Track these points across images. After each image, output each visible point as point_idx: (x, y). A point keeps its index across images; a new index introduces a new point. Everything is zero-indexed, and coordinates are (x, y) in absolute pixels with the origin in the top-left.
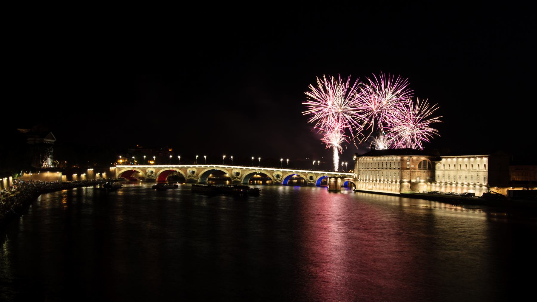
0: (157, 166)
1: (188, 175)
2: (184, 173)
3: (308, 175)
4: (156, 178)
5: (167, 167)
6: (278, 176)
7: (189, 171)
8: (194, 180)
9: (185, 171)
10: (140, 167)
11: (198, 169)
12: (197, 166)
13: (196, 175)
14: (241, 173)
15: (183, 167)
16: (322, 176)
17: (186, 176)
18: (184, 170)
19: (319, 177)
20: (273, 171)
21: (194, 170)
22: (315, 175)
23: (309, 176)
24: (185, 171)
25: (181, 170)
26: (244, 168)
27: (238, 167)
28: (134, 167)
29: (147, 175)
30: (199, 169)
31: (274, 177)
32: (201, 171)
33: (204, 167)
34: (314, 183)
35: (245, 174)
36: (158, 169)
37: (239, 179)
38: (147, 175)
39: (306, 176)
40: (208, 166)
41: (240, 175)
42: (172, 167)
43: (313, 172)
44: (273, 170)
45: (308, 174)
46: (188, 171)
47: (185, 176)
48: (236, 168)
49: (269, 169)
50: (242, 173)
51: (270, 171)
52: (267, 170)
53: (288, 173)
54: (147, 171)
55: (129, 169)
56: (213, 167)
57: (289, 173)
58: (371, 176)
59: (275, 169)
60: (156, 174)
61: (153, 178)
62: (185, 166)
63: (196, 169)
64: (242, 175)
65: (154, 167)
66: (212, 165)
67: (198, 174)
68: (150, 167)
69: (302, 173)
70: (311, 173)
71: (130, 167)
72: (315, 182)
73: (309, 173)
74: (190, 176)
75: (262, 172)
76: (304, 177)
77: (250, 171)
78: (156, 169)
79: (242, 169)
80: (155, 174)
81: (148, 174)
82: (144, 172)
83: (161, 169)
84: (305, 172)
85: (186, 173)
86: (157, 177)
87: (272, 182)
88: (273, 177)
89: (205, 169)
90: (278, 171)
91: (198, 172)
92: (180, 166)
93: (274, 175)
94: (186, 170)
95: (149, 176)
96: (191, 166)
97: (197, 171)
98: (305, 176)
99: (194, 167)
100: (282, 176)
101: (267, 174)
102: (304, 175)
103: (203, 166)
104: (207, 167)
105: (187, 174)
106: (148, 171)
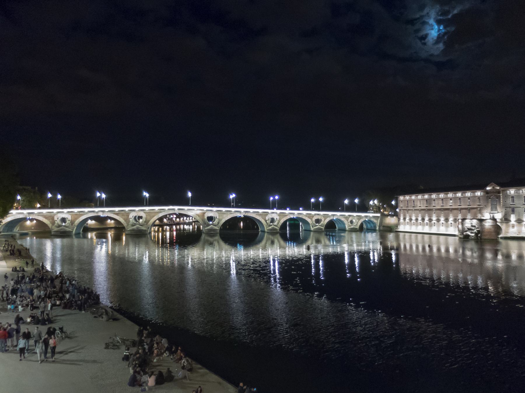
0: (76, 210)
1: (130, 223)
2: (124, 219)
3: (314, 217)
4: (73, 230)
5: (93, 212)
6: (273, 220)
7: (132, 215)
8: (143, 230)
9: (126, 217)
10: (42, 213)
11: (148, 213)
12: (147, 208)
13: (145, 222)
14: (218, 218)
15: (122, 211)
16: (332, 218)
17: (128, 225)
18: (123, 215)
19: (328, 220)
20: (265, 214)
21: (142, 214)
22: (323, 216)
23: (316, 218)
24: (126, 217)
25: (118, 215)
26: (224, 209)
27: (215, 209)
28: (29, 213)
29: (56, 224)
30: (151, 214)
31: (267, 221)
32: (154, 216)
33: (159, 210)
34: (322, 227)
35: (223, 218)
36: (76, 214)
37: (215, 226)
38: (56, 224)
39: (312, 220)
40: (166, 208)
41: (216, 222)
42: (103, 211)
43: (322, 213)
44: (268, 212)
45: (313, 216)
46: (132, 217)
47: (125, 224)
48: (211, 210)
49: (261, 211)
50: (221, 217)
51: (262, 214)
52: (258, 212)
53: (286, 216)
54: (56, 218)
55: (21, 216)
56: (174, 209)
57: (288, 216)
58: (414, 214)
59: (269, 211)
60: (72, 222)
61: (68, 229)
62: (127, 209)
63: (144, 212)
64: (220, 220)
65: (68, 212)
66: (171, 207)
67: (149, 221)
68: (63, 212)
69: (323, 216)
70: (318, 214)
71: (22, 213)
72: (323, 226)
73: (315, 214)
74: (133, 225)
75: (249, 215)
76: (309, 220)
77: (232, 213)
78: (72, 215)
79: (220, 212)
80: (71, 222)
81: (58, 223)
82: (51, 220)
83: (82, 215)
84: (310, 214)
85: (127, 220)
86: (74, 228)
87: (199, 228)
88: (266, 221)
89: (161, 212)
90: (273, 213)
91: (148, 218)
92: (117, 209)
93: (267, 218)
94: (128, 216)
95: (59, 226)
96: (137, 209)
97: (146, 215)
98: (310, 218)
99: (142, 210)
100: (278, 219)
101: (258, 218)
102: (309, 217)
103: (157, 208)
104: (163, 209)
105: (129, 221)
106: (58, 218)
